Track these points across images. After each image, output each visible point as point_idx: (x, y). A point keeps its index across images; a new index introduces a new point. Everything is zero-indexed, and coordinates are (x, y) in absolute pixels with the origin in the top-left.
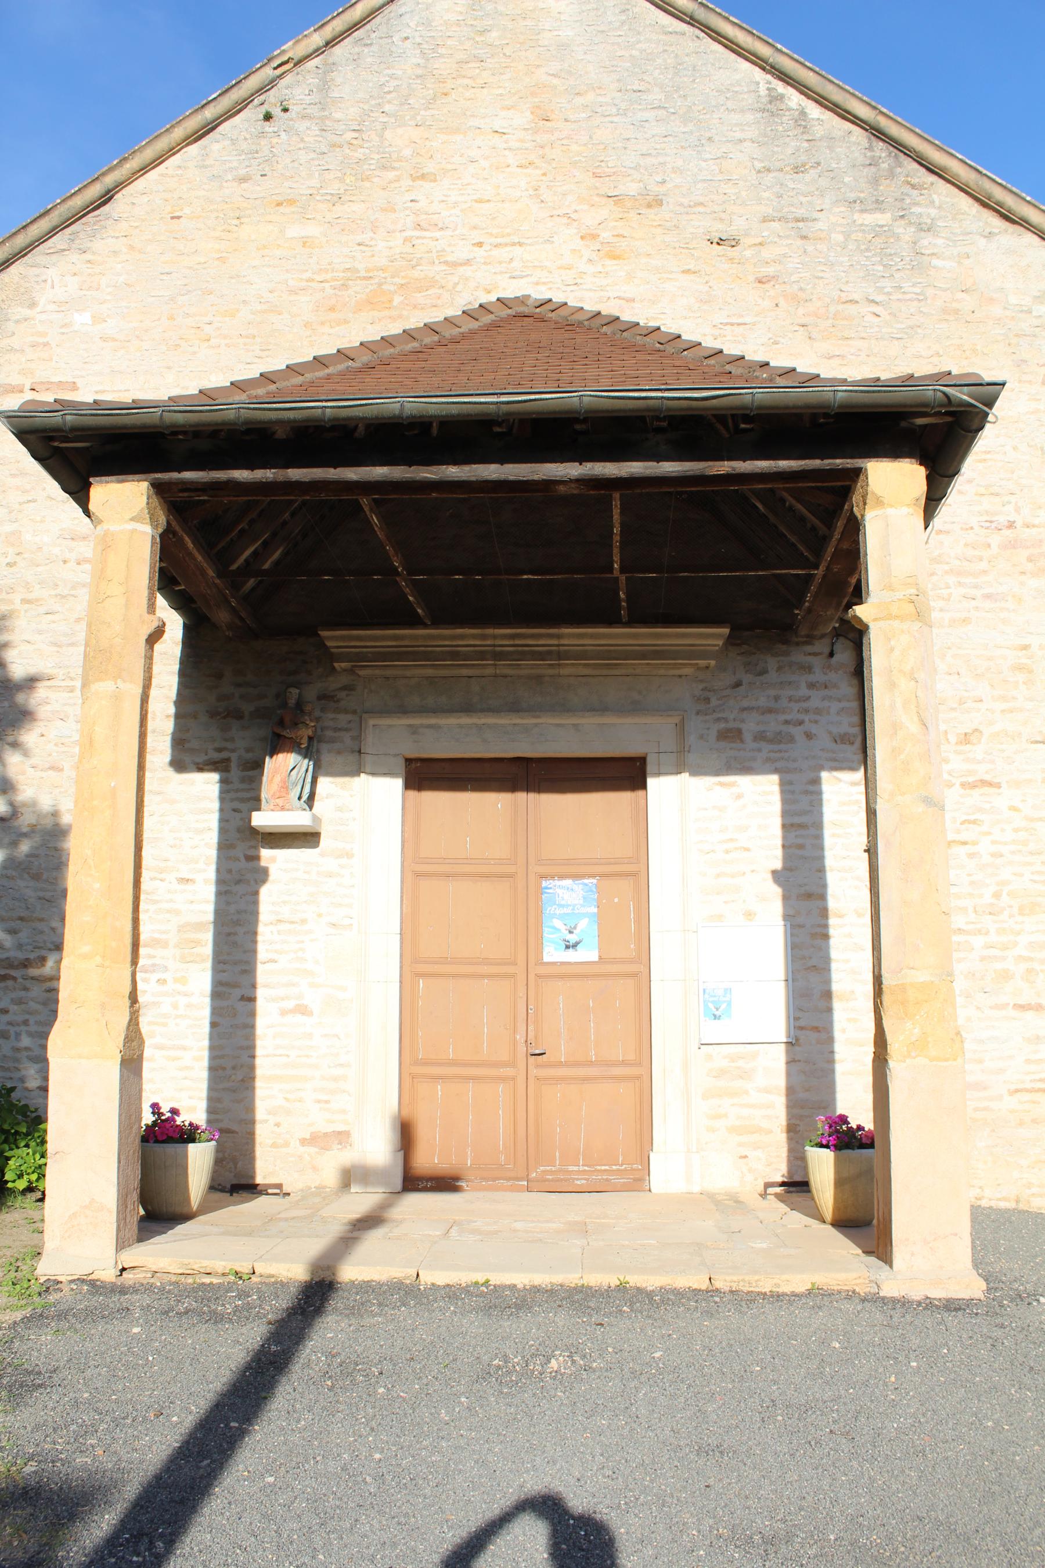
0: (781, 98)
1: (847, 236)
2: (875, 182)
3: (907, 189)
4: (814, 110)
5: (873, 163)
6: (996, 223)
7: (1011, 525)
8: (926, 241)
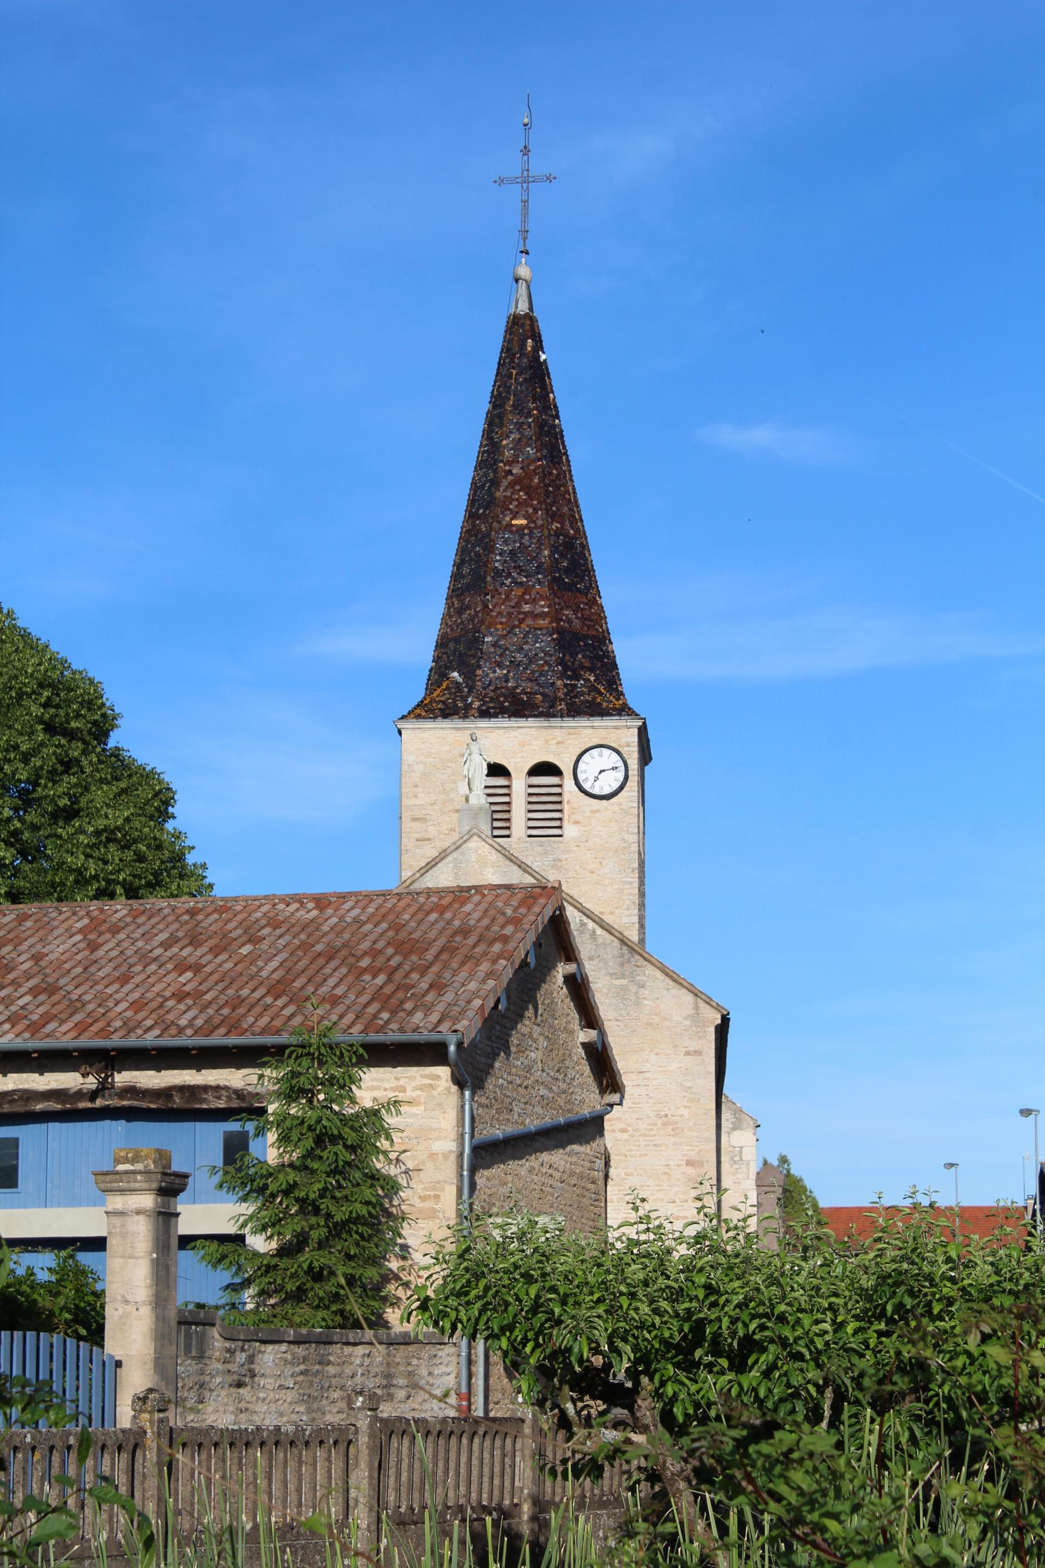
0: (585, 924)
1: (609, 990)
2: (622, 965)
3: (635, 968)
4: (599, 931)
5: (622, 955)
6: (671, 983)
7: (666, 1116)
8: (641, 991)
